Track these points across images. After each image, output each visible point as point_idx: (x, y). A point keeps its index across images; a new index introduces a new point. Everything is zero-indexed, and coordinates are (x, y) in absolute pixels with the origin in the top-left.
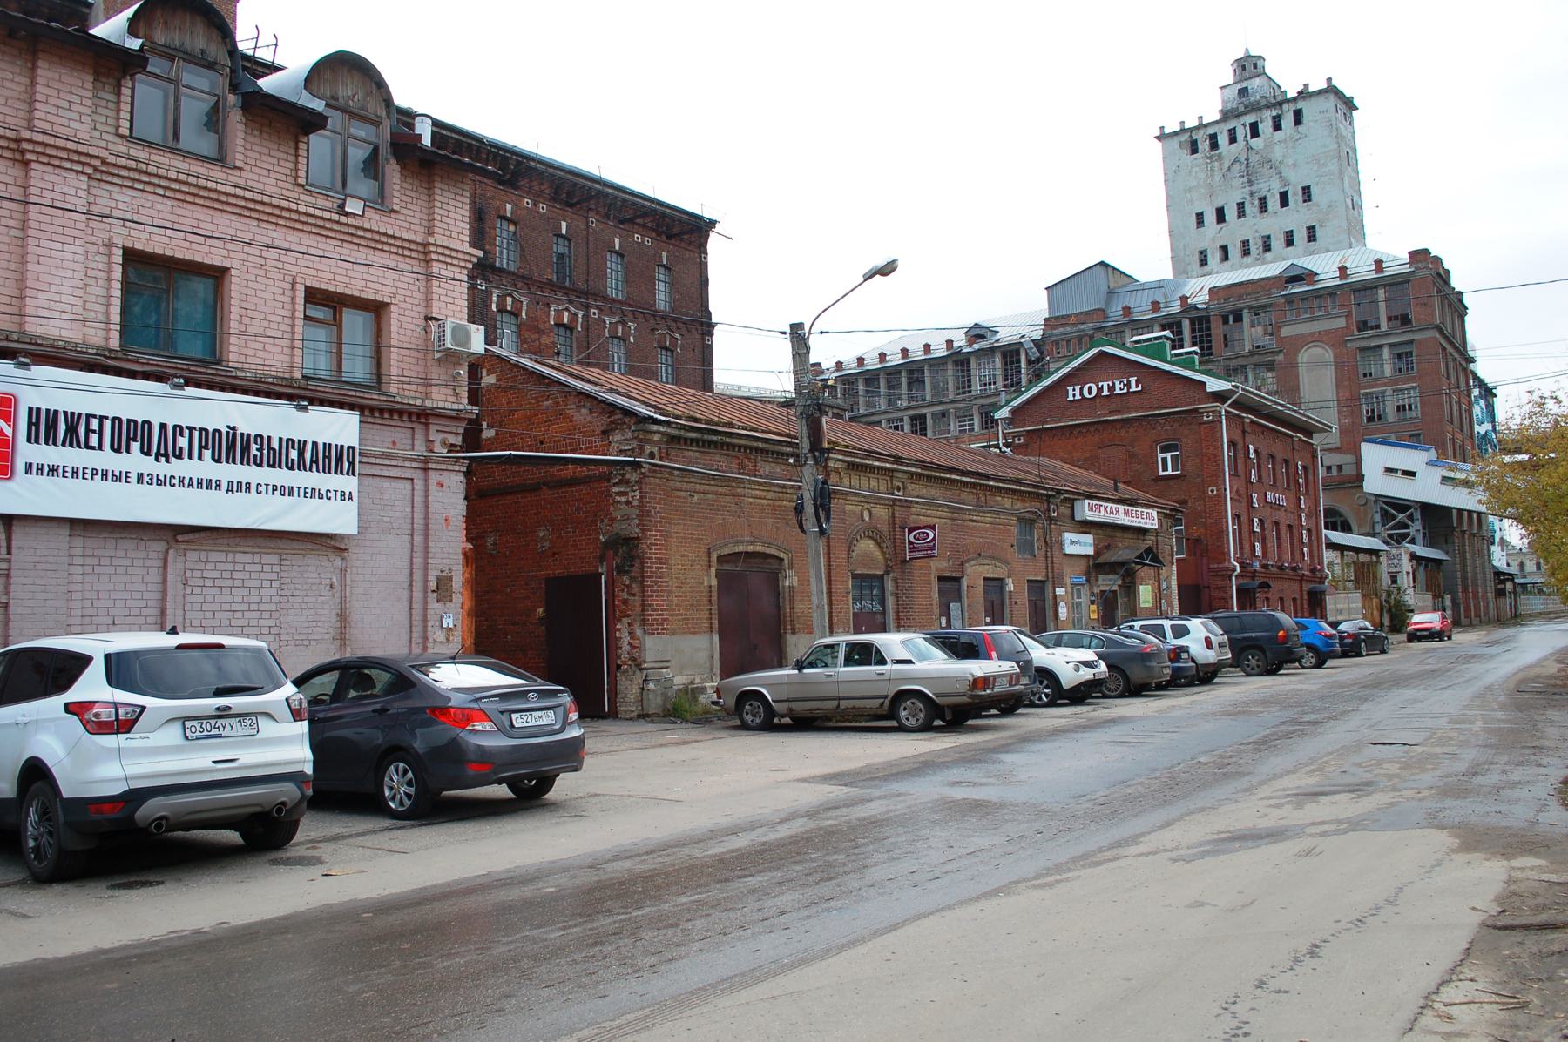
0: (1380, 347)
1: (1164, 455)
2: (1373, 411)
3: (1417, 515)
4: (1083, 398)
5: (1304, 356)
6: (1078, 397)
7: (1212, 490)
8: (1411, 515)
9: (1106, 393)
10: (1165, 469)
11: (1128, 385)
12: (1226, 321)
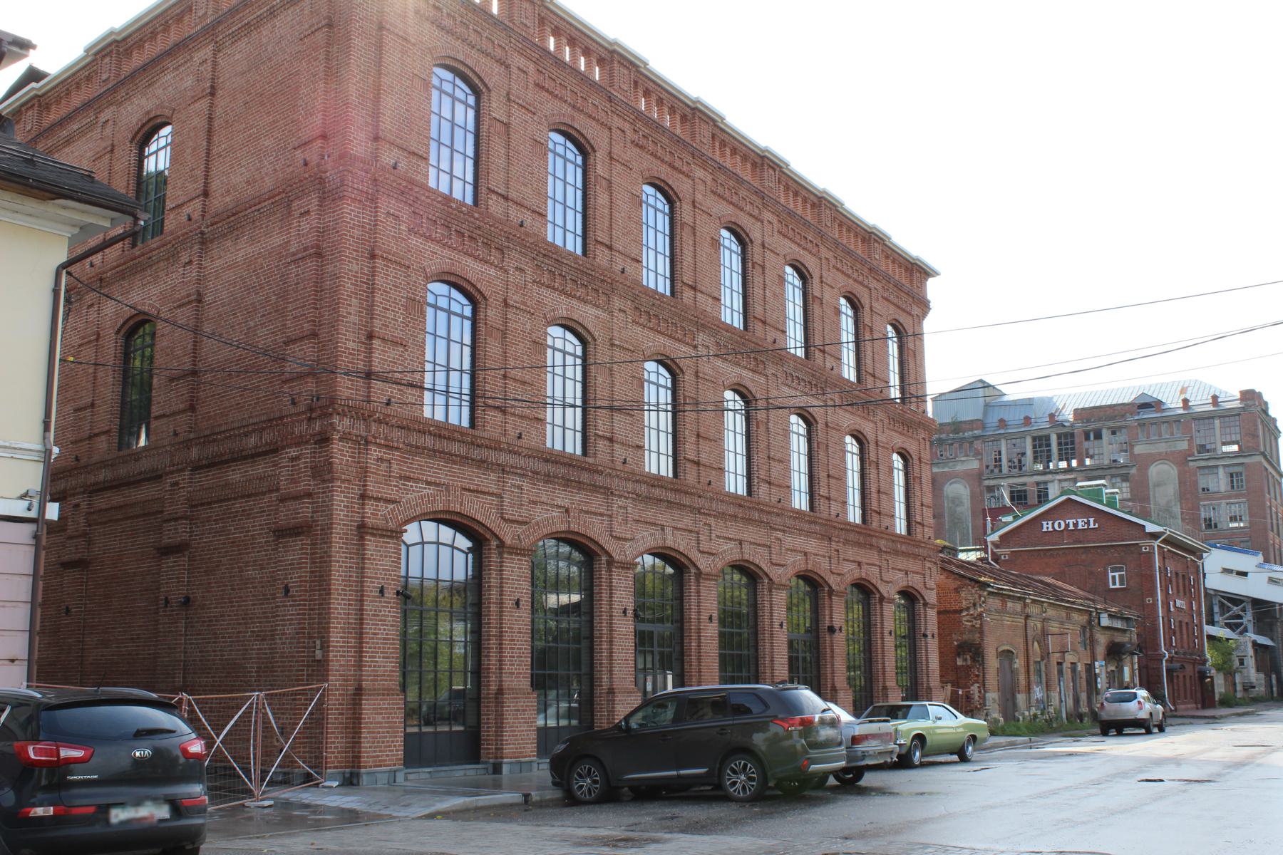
0: (1217, 467)
1: (1113, 574)
2: (1210, 519)
3: (1249, 607)
4: (1055, 530)
6: (1050, 529)
7: (1149, 600)
8: (1244, 607)
9: (1071, 527)
10: (1114, 583)
11: (1088, 523)
12: (1087, 438)
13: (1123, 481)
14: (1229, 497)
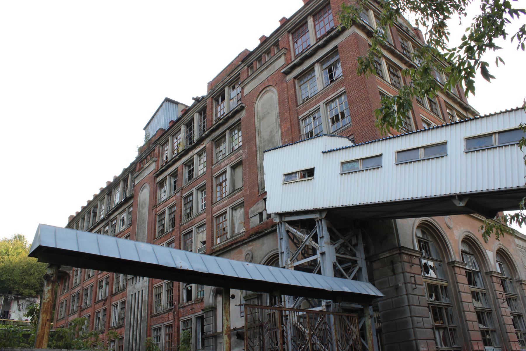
5: (259, 106)
13: (239, 130)
14: (327, 95)
